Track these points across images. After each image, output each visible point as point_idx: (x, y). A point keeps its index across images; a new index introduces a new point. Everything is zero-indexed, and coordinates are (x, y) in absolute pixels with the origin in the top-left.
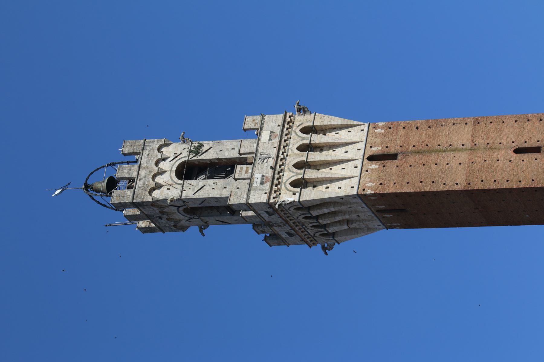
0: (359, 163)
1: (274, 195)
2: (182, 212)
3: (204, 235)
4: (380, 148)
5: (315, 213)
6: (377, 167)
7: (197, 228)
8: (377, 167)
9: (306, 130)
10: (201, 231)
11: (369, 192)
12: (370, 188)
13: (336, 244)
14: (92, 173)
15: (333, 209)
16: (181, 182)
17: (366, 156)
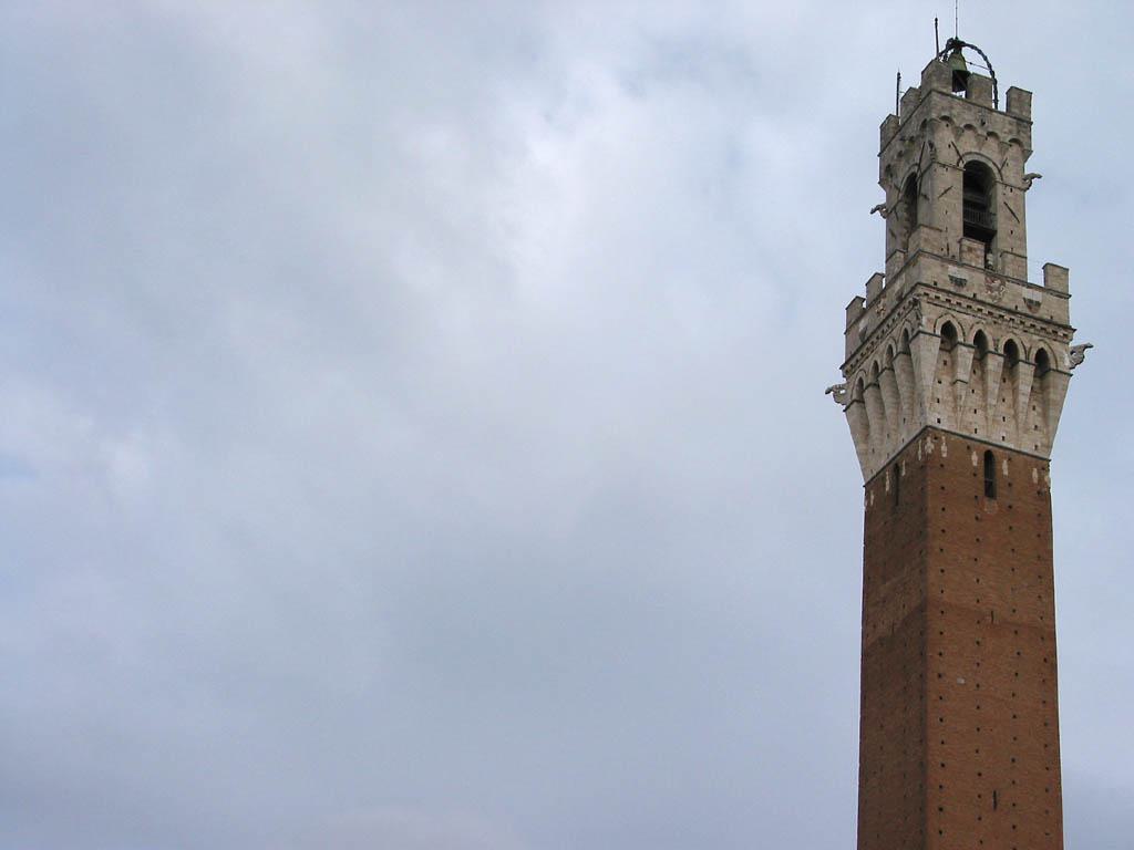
0: (980, 435)
1: (933, 294)
2: (912, 170)
3: (873, 212)
4: (1006, 473)
5: (899, 363)
6: (975, 464)
7: (883, 200)
8: (975, 464)
9: (1042, 357)
10: (878, 208)
11: (930, 446)
12: (937, 449)
13: (844, 407)
14: (980, 52)
15: (904, 391)
16: (961, 165)
17: (990, 447)
